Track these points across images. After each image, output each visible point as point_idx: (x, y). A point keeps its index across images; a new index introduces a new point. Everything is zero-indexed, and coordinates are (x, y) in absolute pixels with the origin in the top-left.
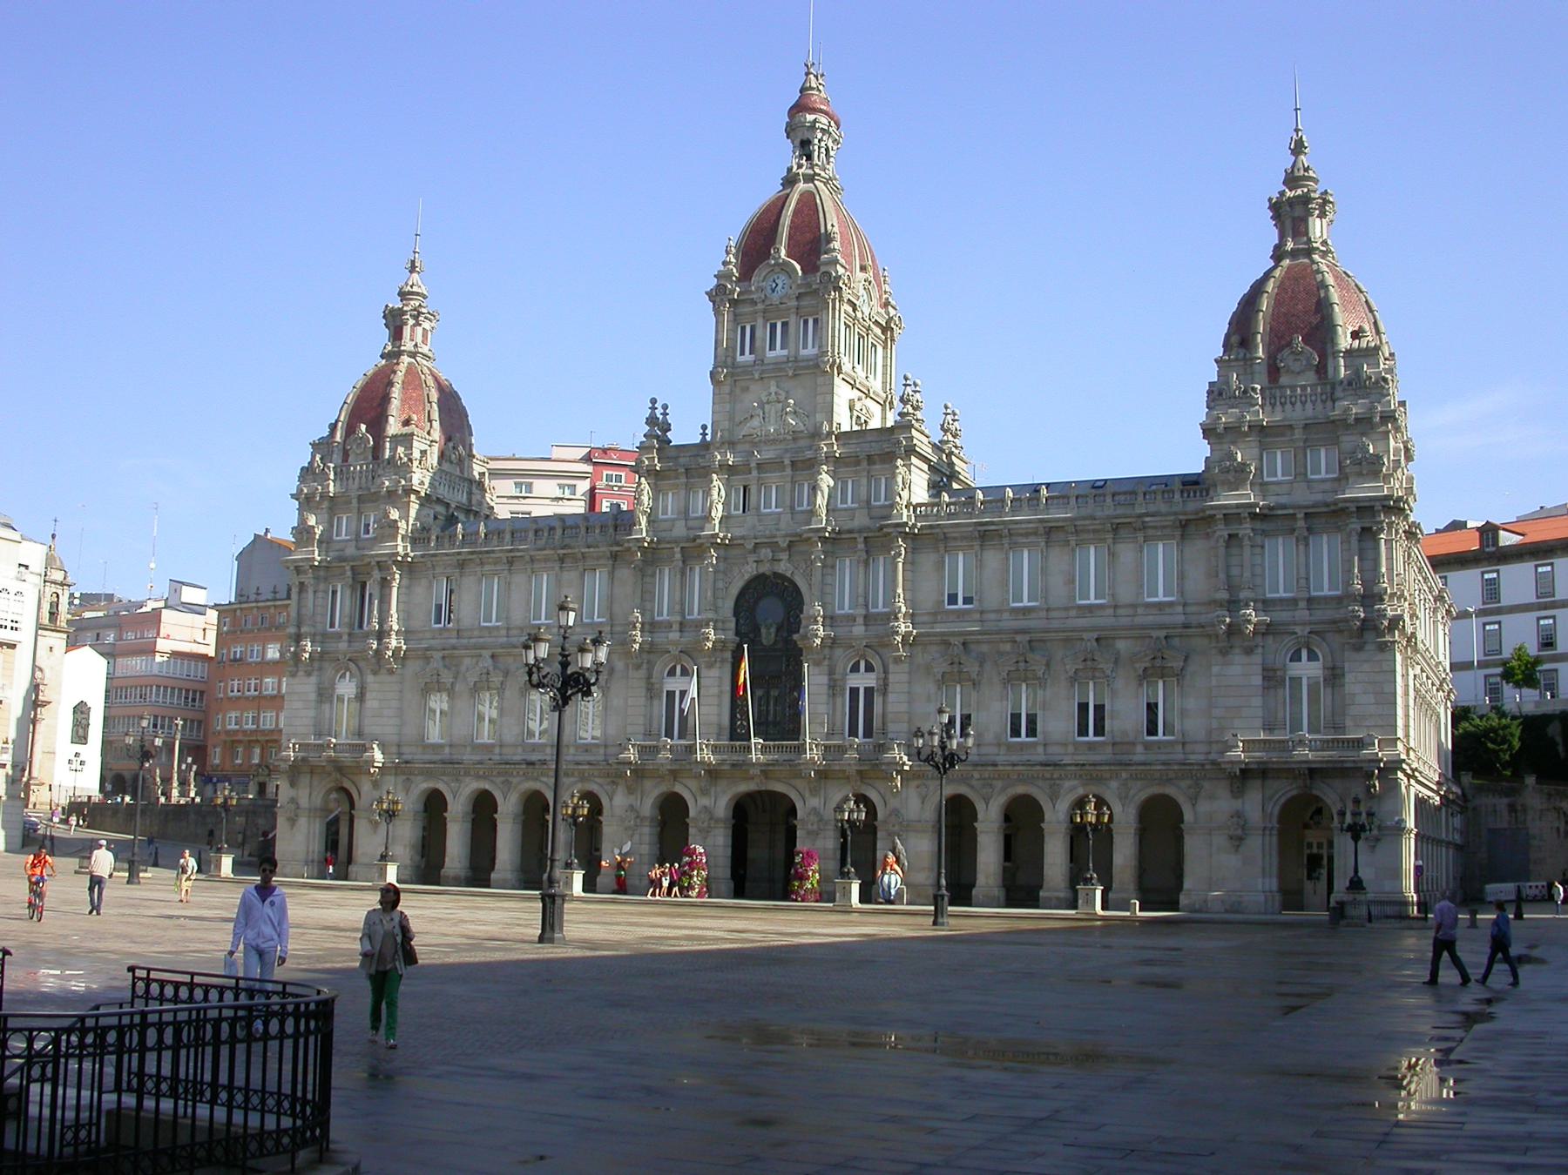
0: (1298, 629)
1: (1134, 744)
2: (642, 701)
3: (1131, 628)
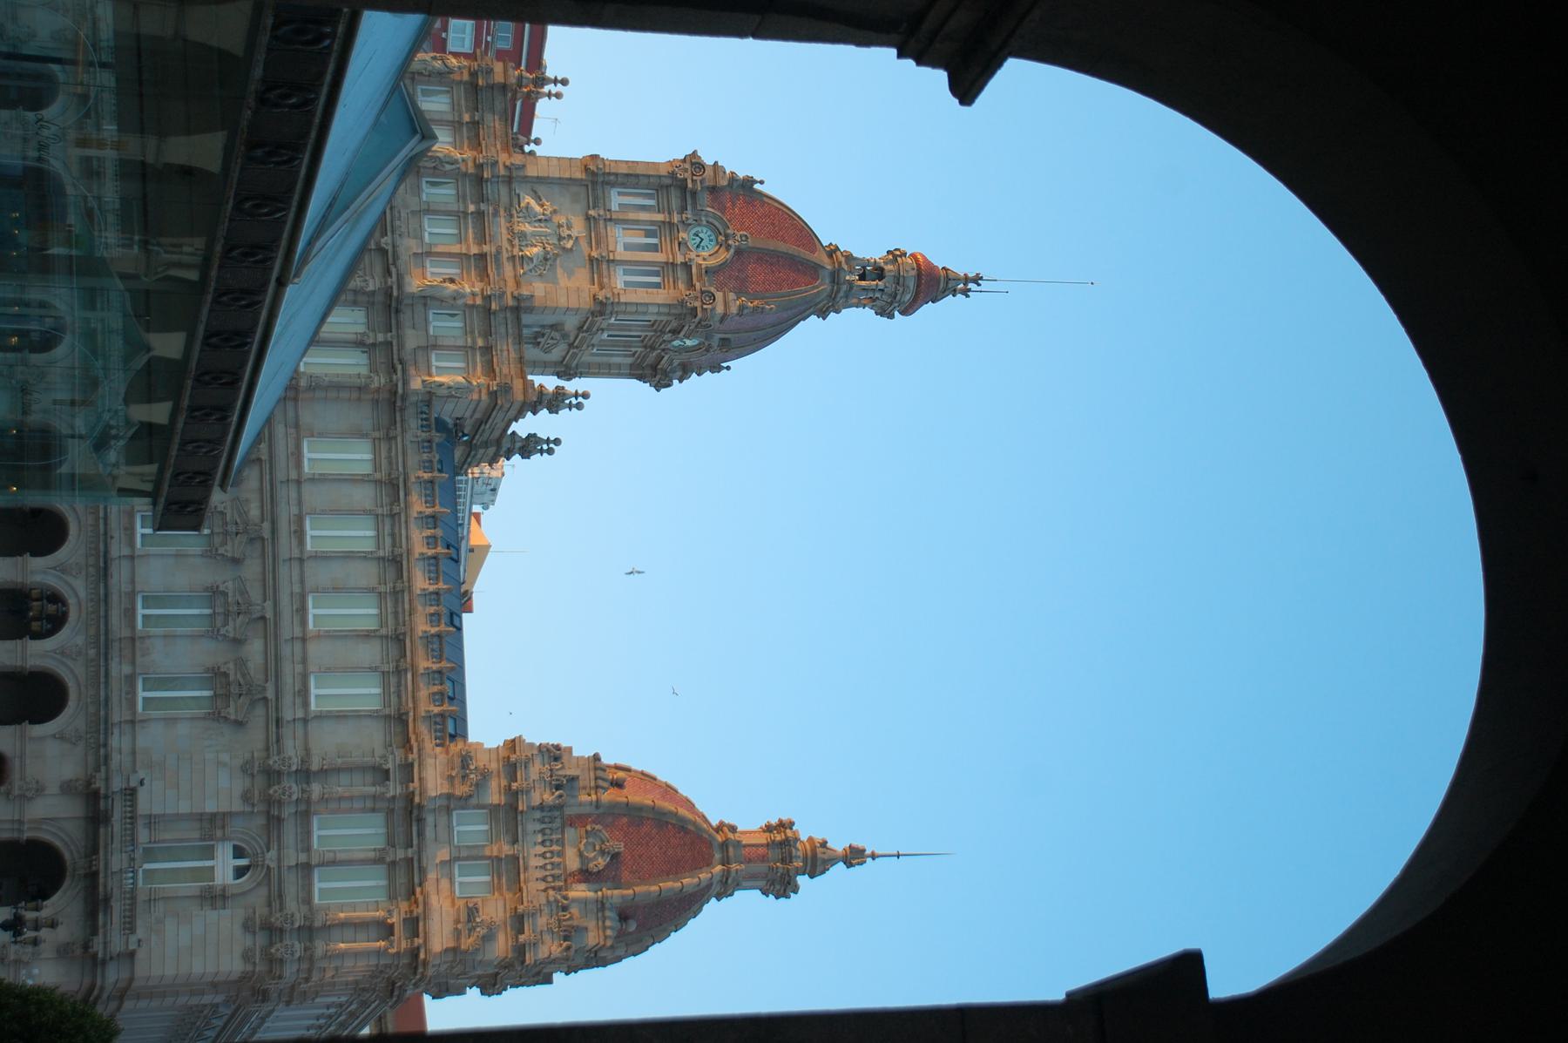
0: (273, 854)
1: (133, 663)
3: (278, 659)
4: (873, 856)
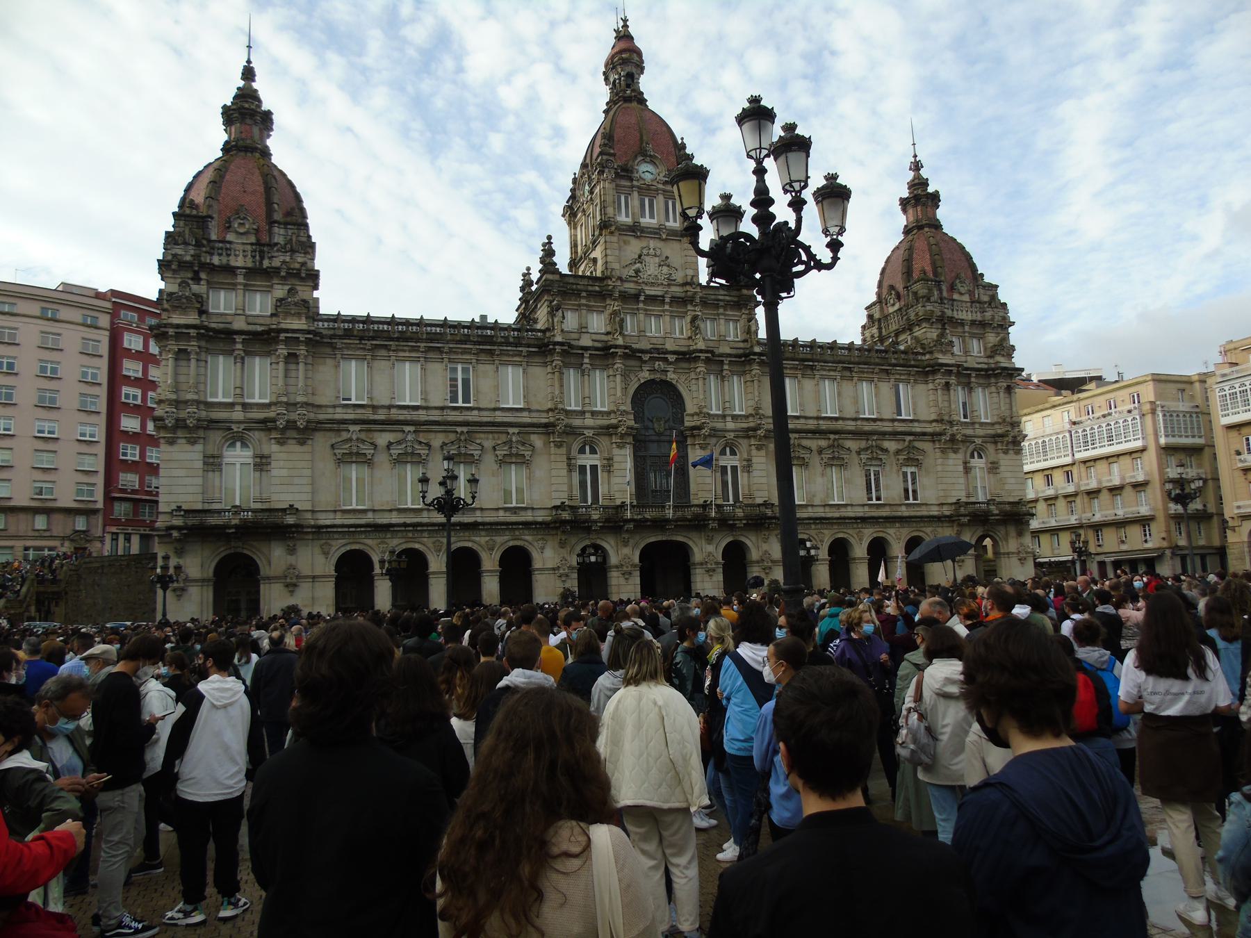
2: (564, 472)
4: (915, 156)
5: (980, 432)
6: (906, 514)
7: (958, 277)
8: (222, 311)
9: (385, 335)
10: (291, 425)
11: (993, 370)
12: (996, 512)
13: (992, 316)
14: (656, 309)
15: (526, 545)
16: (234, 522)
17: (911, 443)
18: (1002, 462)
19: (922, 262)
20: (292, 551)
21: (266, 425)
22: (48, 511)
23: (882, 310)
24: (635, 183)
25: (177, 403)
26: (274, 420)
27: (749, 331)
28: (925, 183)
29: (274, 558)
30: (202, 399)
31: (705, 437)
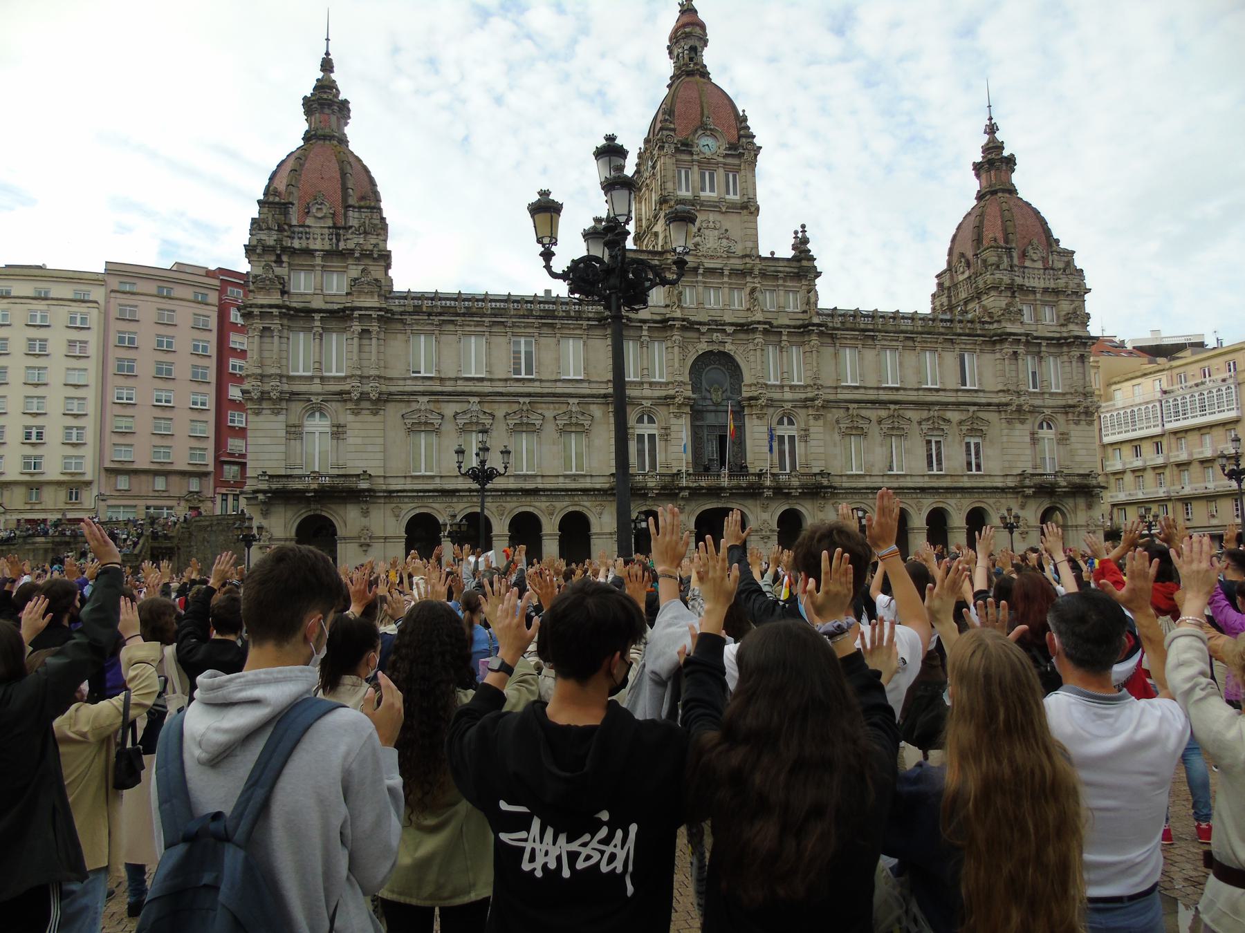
4: (990, 119)
5: (1049, 402)
6: (968, 485)
7: (1030, 243)
8: (302, 291)
9: (452, 310)
10: (364, 397)
11: (1066, 338)
12: (1065, 484)
13: (1067, 284)
14: (714, 281)
15: (585, 511)
16: (313, 486)
17: (975, 413)
18: (1072, 433)
19: (993, 231)
20: (366, 513)
21: (342, 397)
22: (167, 474)
23: (952, 277)
24: (695, 157)
25: (262, 377)
26: (349, 393)
27: (808, 303)
28: (1000, 147)
29: (348, 520)
30: (285, 373)
31: (762, 407)
